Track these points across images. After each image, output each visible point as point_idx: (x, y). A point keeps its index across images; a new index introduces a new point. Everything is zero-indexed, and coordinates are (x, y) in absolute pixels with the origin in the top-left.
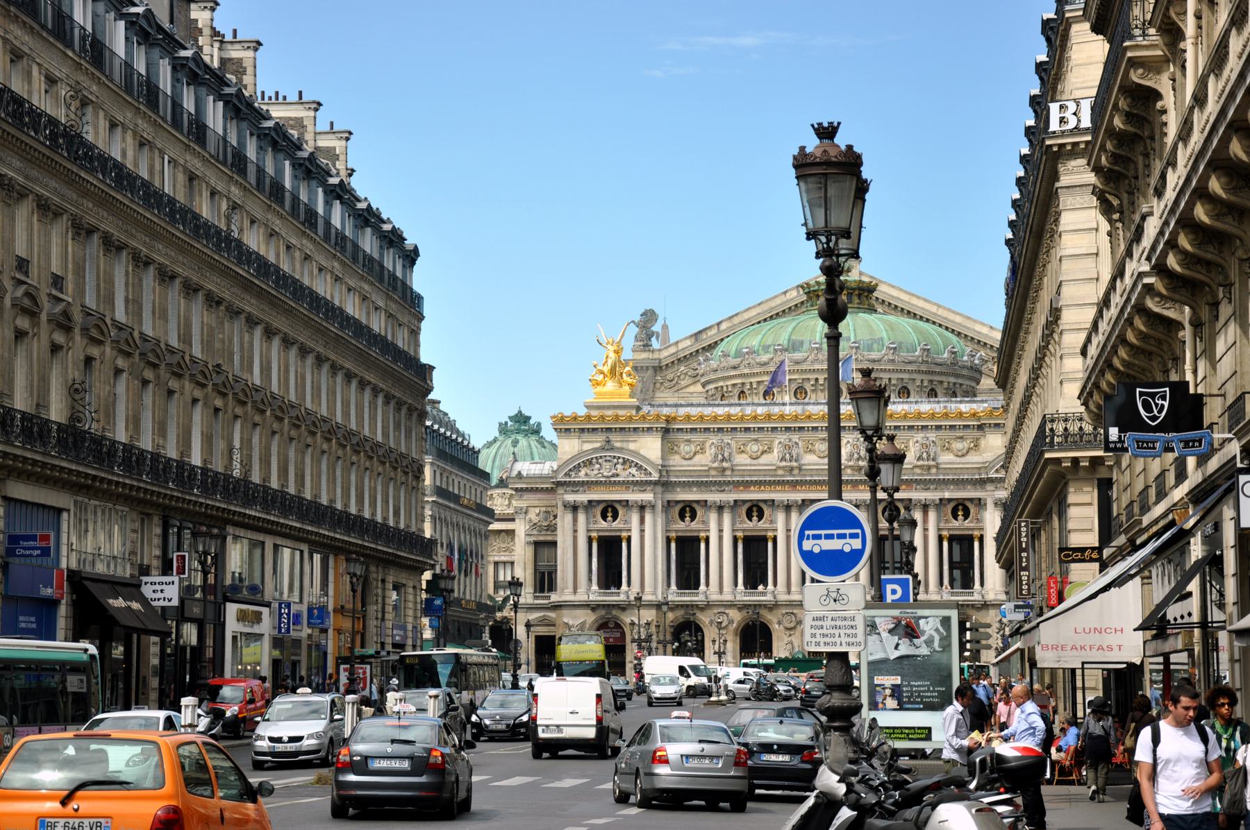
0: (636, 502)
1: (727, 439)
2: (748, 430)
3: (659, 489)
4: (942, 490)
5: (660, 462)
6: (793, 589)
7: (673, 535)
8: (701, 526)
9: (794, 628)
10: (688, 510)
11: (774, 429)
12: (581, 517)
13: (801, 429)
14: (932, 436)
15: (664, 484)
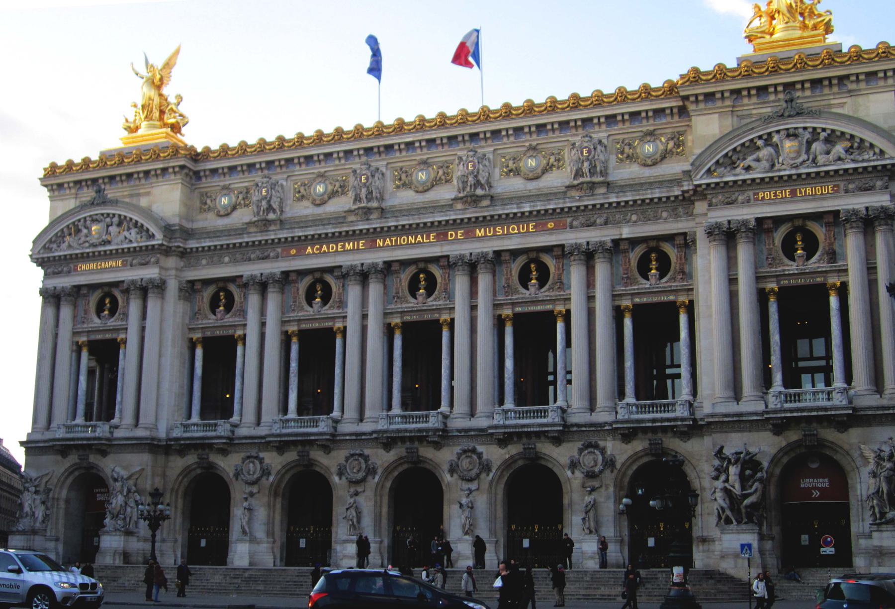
0: (133, 282)
1: (279, 177)
2: (309, 159)
3: (172, 262)
4: (617, 223)
5: (176, 221)
6: (368, 413)
7: (197, 335)
8: (237, 320)
9: (363, 480)
10: (223, 295)
11: (348, 153)
12: (66, 312)
13: (389, 148)
14: (600, 133)
15: (184, 254)
